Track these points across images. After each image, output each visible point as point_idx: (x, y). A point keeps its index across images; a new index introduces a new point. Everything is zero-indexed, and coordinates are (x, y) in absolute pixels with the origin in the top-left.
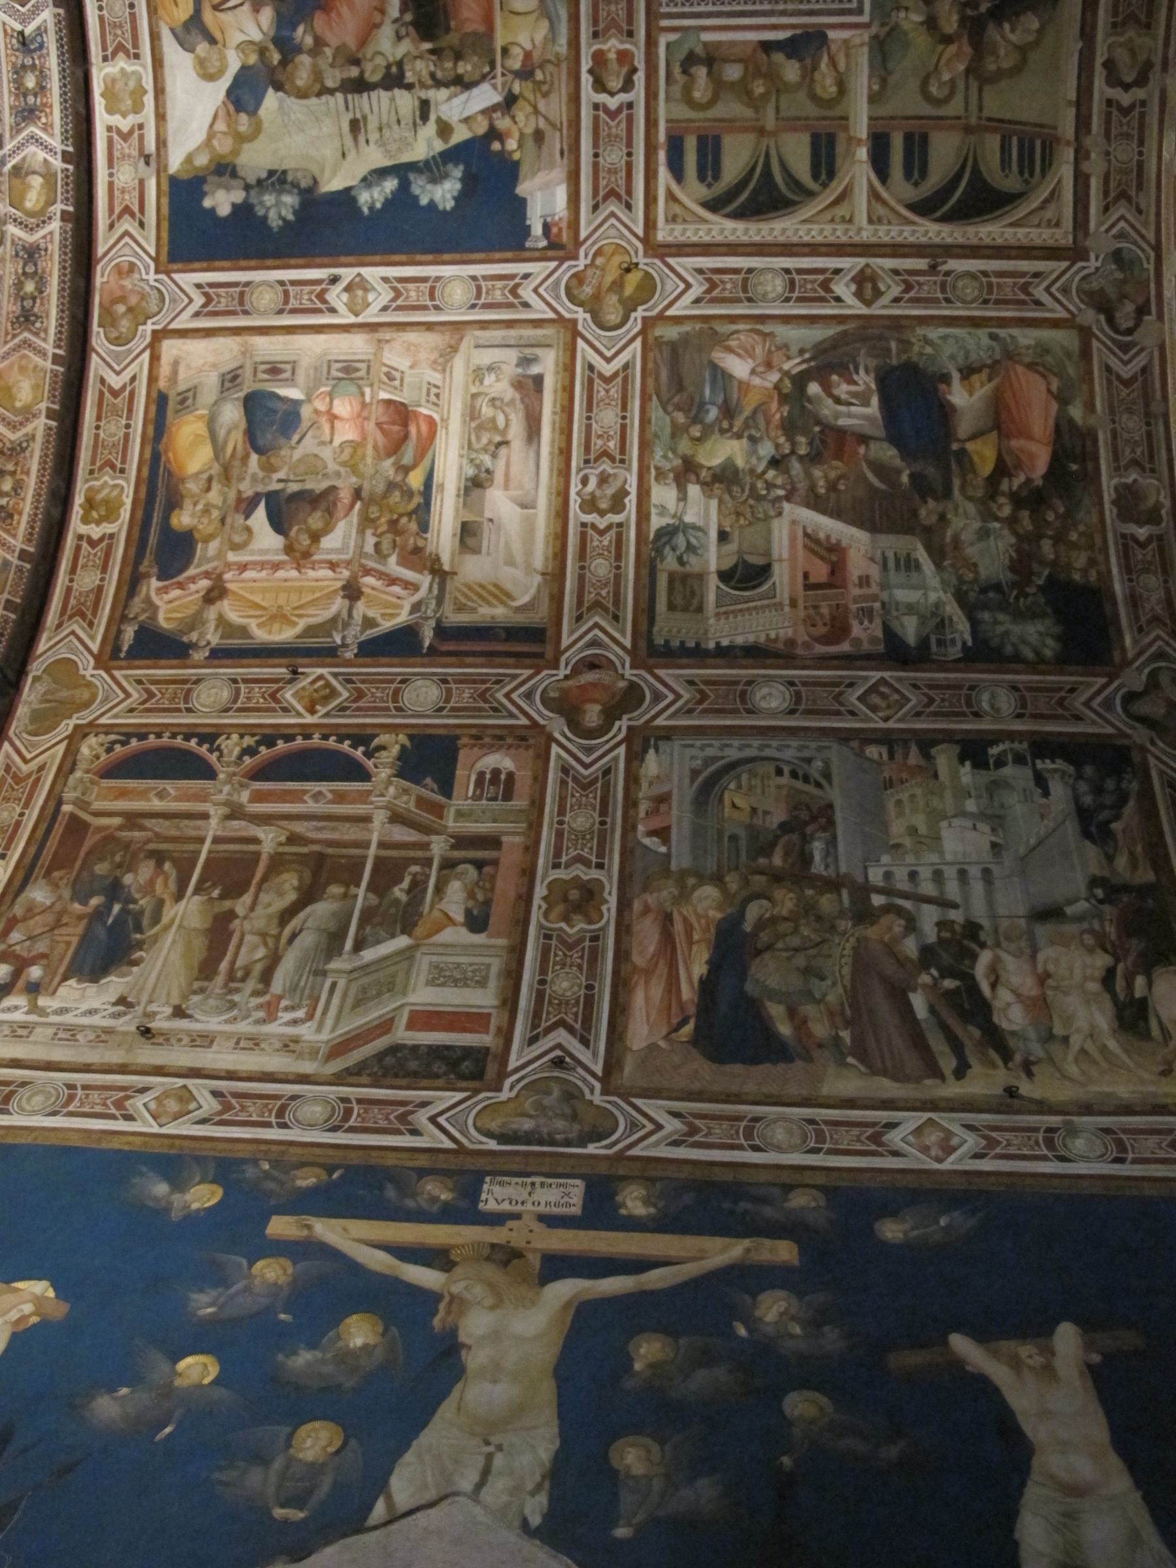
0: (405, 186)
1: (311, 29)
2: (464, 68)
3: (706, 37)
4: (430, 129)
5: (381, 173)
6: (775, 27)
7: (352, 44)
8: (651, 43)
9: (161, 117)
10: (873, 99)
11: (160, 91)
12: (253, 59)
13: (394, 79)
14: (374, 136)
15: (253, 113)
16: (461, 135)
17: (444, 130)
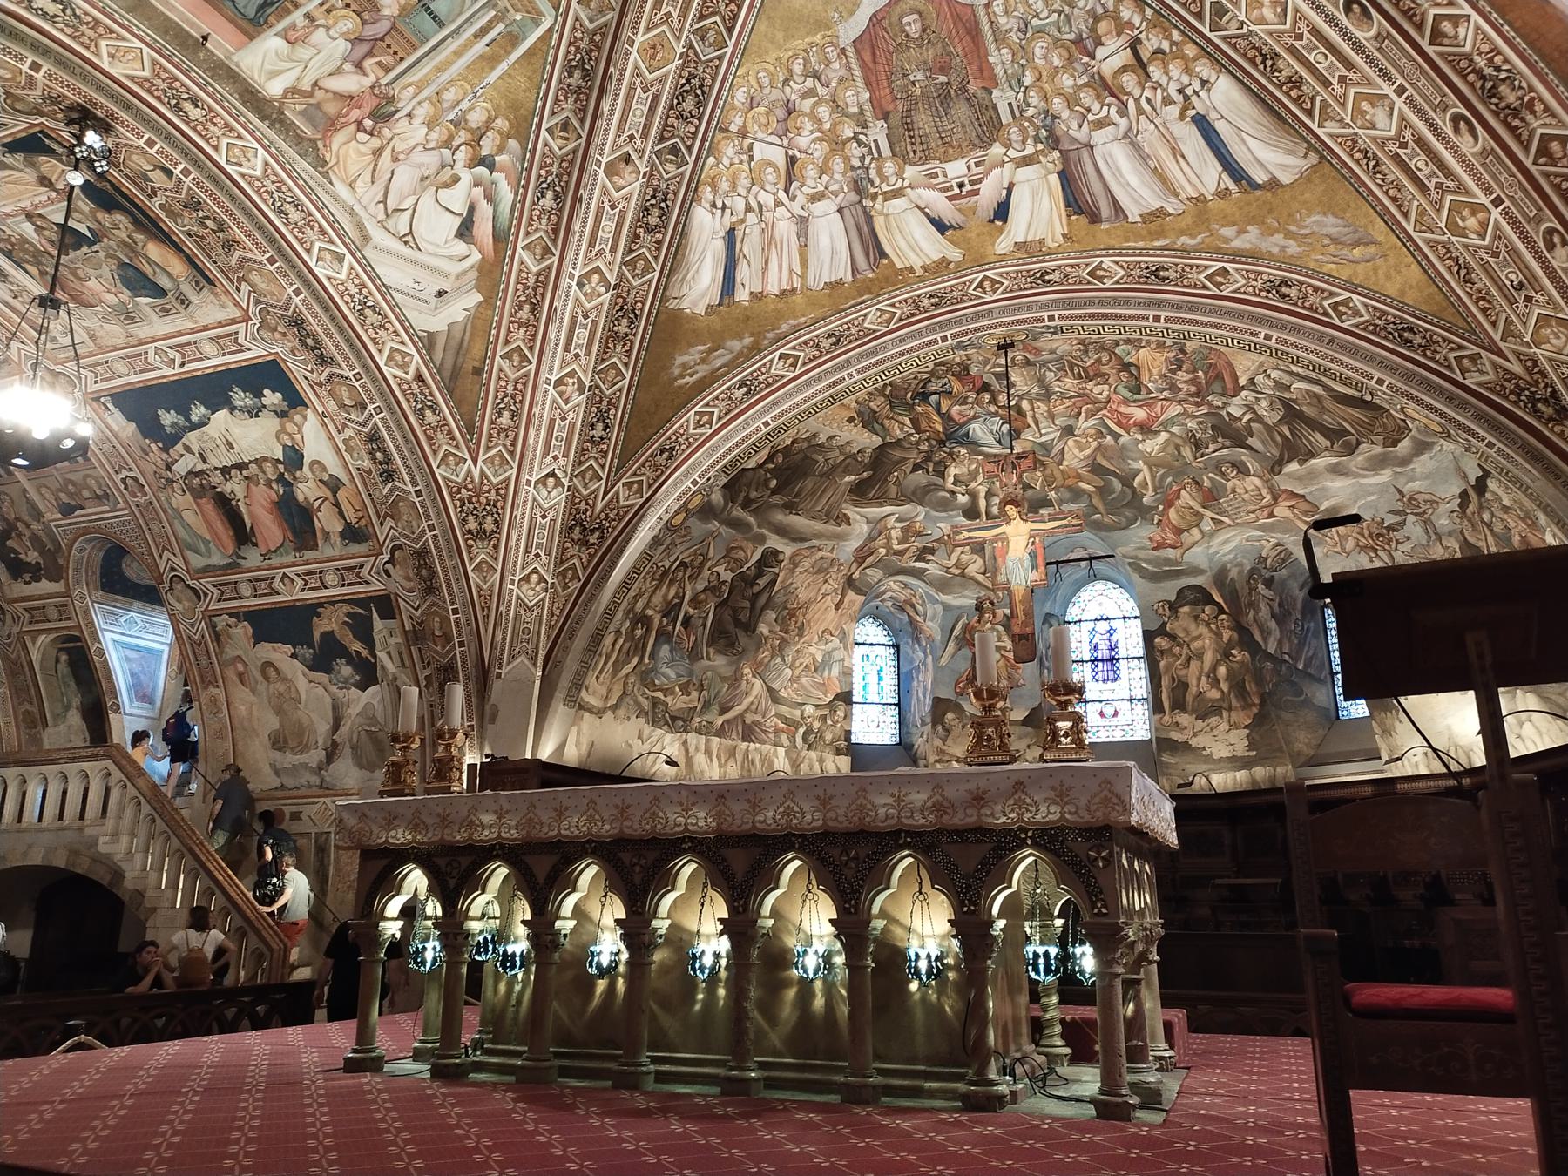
0: (188, 419)
1: (277, 492)
2: (197, 481)
3: (106, 508)
4: (195, 448)
5: (203, 423)
6: (82, 516)
7: (253, 487)
8: (126, 502)
9: (331, 438)
10: (25, 490)
11: (338, 451)
12: (298, 474)
13: (225, 471)
14: (218, 442)
15: (285, 446)
16: (179, 447)
17: (188, 449)
